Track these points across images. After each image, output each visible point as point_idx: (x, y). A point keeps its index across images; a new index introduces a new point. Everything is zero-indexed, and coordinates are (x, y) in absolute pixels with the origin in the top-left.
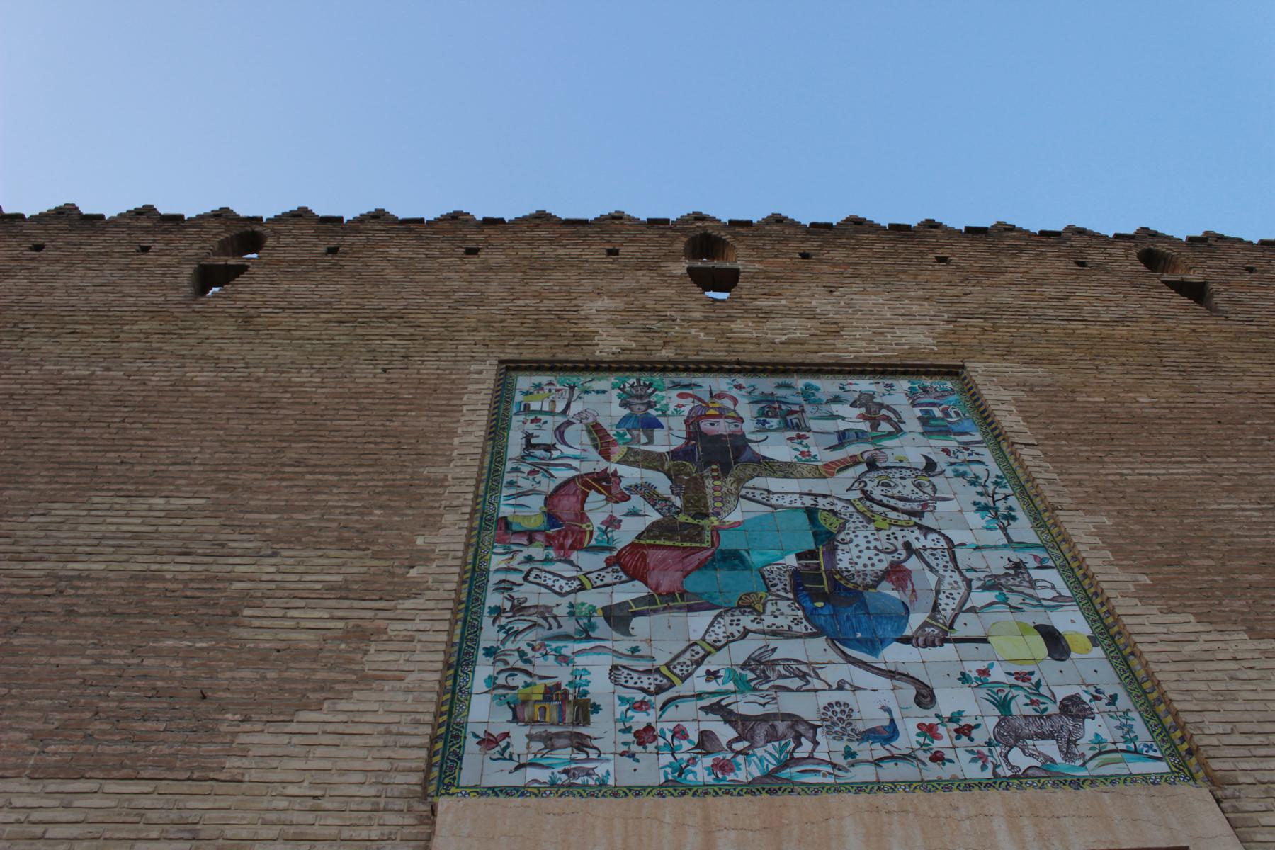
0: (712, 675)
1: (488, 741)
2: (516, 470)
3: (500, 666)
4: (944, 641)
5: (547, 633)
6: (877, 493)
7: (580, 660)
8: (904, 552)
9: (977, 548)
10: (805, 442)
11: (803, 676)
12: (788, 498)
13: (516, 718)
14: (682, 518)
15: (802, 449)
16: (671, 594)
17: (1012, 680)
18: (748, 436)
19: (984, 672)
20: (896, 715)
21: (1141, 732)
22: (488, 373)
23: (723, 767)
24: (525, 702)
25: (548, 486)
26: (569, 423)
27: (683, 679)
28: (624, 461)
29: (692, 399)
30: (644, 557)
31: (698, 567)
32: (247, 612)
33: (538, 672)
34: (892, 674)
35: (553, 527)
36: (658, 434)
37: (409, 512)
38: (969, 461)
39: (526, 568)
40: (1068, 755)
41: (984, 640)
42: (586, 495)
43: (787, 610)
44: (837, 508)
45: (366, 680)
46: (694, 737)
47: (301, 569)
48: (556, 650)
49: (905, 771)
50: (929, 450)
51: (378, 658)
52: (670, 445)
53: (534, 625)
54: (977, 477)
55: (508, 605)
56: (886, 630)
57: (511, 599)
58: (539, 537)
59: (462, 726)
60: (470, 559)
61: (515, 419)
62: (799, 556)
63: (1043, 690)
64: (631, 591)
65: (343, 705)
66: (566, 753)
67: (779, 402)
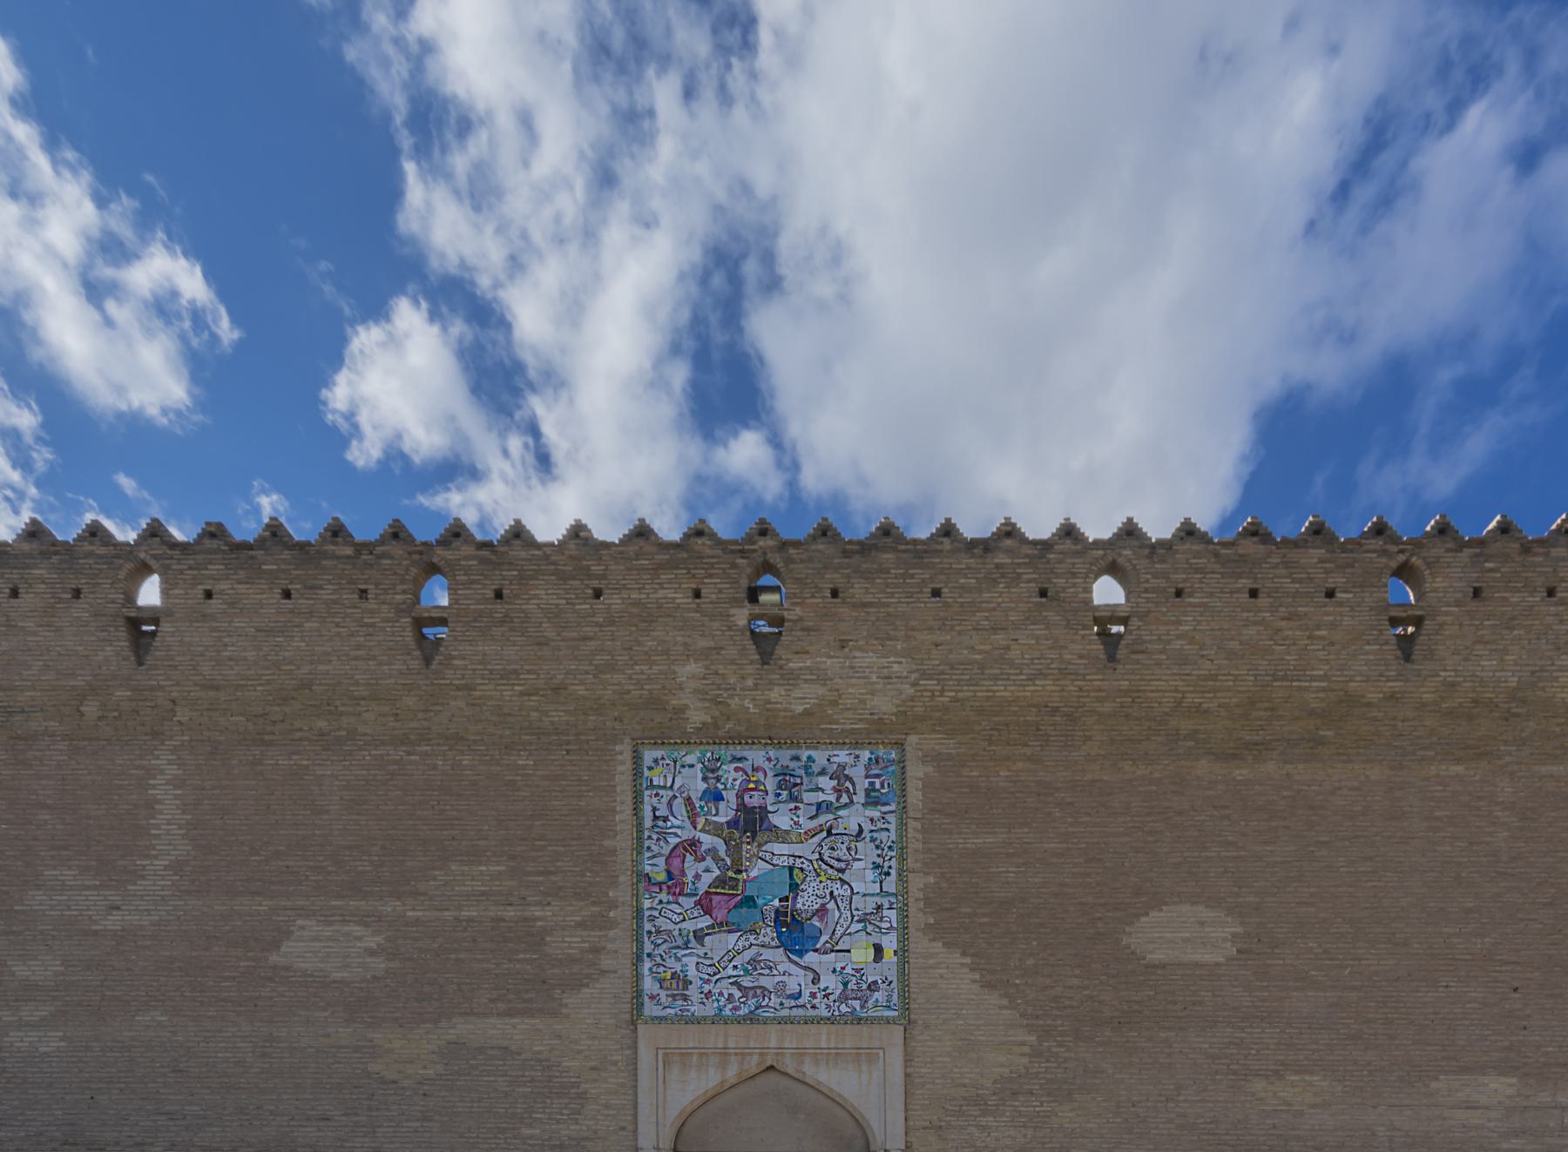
0: (735, 967)
1: (652, 997)
2: (650, 837)
3: (653, 963)
4: (832, 951)
5: (671, 945)
6: (826, 854)
7: (684, 959)
8: (828, 897)
9: (865, 895)
10: (798, 812)
11: (770, 968)
12: (782, 858)
13: (661, 987)
14: (730, 874)
15: (796, 819)
16: (722, 923)
17: (853, 972)
18: (770, 808)
19: (843, 968)
20: (803, 988)
21: (895, 996)
22: (624, 750)
23: (736, 1009)
24: (664, 980)
25: (666, 850)
26: (675, 797)
27: (724, 969)
28: (702, 831)
29: (741, 773)
30: (711, 900)
31: (735, 907)
32: (548, 939)
33: (667, 965)
34: (806, 968)
35: (670, 880)
36: (722, 805)
37: (603, 874)
38: (882, 829)
39: (659, 907)
40: (862, 1007)
41: (849, 951)
42: (685, 856)
43: (769, 932)
44: (804, 866)
45: (603, 972)
46: (726, 996)
47: (562, 913)
48: (675, 954)
49: (800, 1012)
50: (862, 819)
51: (606, 962)
52: (727, 816)
53: (665, 941)
54: (881, 842)
55: (653, 930)
56: (809, 946)
57: (655, 926)
58: (664, 887)
59: (642, 990)
60: (635, 903)
61: (647, 793)
62: (780, 900)
63: (864, 978)
64: (705, 922)
65: (597, 986)
66: (680, 1002)
67: (791, 775)
